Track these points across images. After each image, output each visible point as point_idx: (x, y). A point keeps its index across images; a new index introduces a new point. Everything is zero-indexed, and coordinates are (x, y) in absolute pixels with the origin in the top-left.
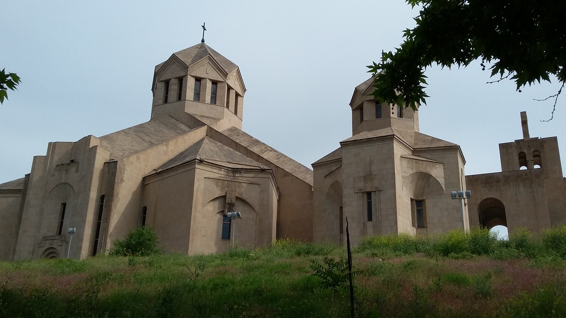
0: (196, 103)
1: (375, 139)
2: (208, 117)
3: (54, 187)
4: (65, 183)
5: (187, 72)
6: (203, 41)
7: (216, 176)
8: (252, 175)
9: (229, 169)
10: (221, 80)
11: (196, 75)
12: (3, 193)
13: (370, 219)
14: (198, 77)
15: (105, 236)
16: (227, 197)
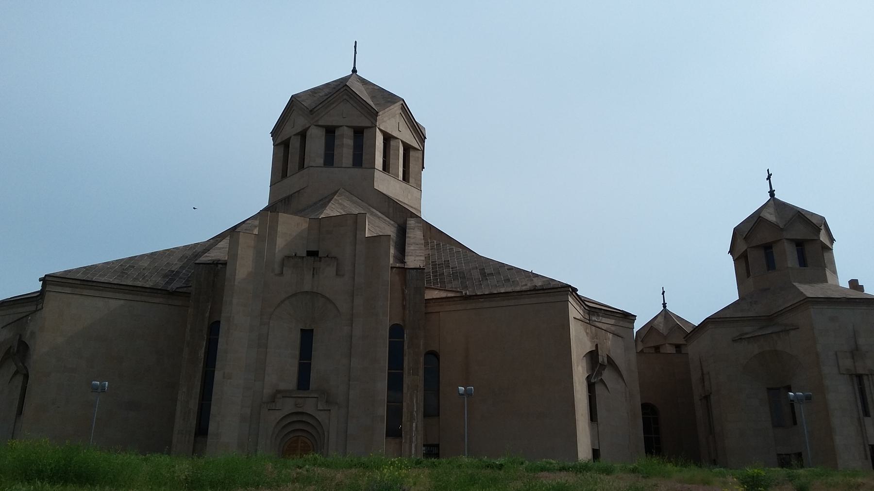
0: (384, 176)
1: (857, 300)
2: (405, 203)
3: (288, 298)
4: (313, 294)
5: (374, 121)
6: (354, 71)
7: (579, 316)
8: (612, 321)
9: (587, 308)
10: (416, 146)
11: (386, 130)
12: (96, 288)
13: (867, 413)
14: (388, 133)
15: (417, 401)
16: (600, 352)
